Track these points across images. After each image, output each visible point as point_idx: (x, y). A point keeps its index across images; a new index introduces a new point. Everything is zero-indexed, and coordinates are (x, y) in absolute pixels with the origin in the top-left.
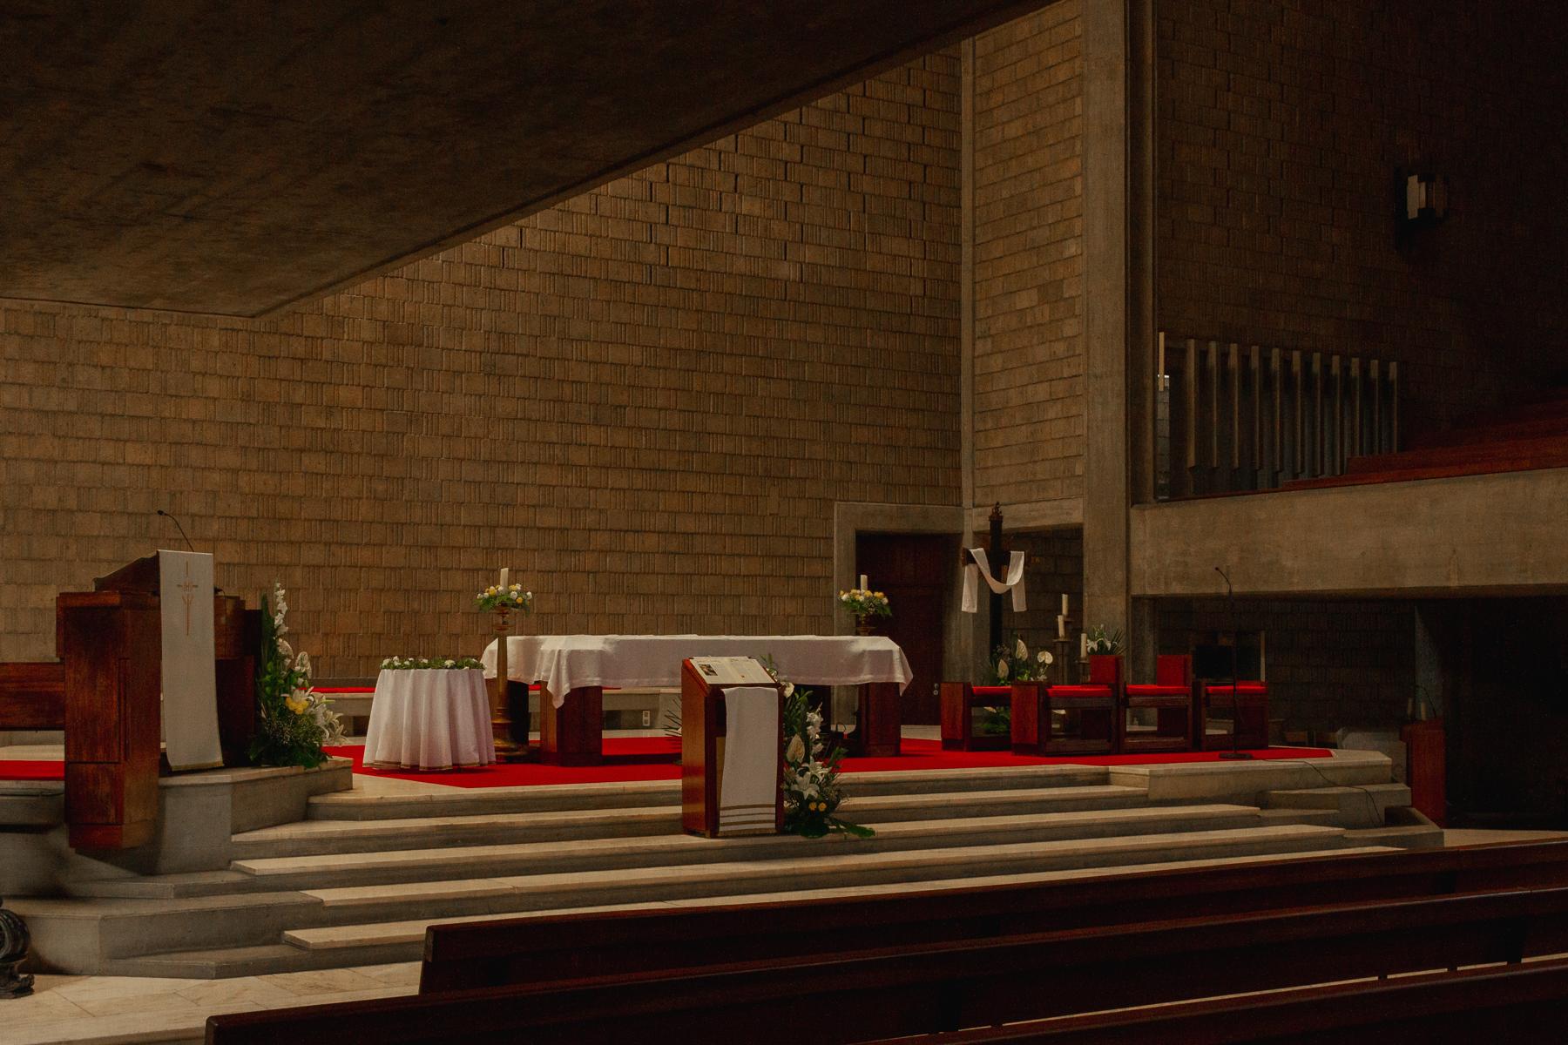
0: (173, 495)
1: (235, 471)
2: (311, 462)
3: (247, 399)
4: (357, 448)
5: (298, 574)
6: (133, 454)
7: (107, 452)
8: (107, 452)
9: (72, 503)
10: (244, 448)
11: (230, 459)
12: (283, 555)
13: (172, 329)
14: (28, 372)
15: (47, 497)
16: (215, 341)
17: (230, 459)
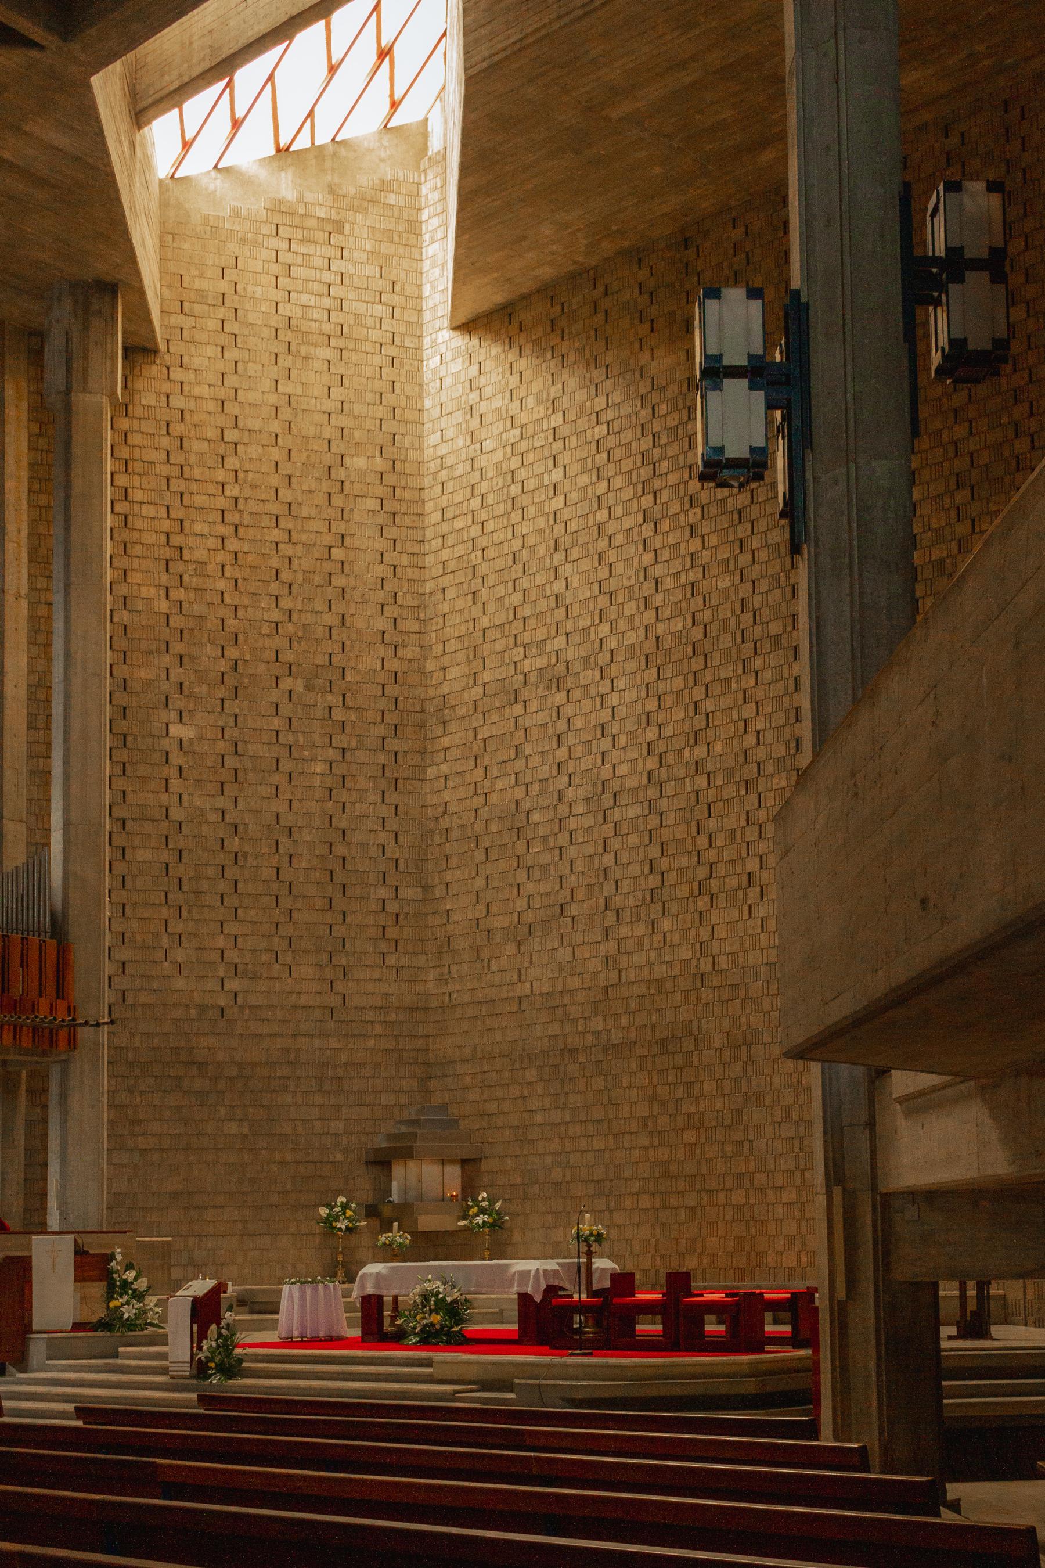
0: (616, 1167)
1: (646, 1148)
2: (690, 1136)
3: (652, 1099)
4: (714, 1123)
5: (682, 1214)
6: (598, 1144)
7: (584, 1144)
8: (584, 1144)
9: (568, 1178)
10: (651, 1133)
11: (644, 1141)
12: (674, 1202)
13: (613, 1062)
14: (547, 1101)
15: (557, 1175)
16: (634, 1065)
17: (644, 1141)
